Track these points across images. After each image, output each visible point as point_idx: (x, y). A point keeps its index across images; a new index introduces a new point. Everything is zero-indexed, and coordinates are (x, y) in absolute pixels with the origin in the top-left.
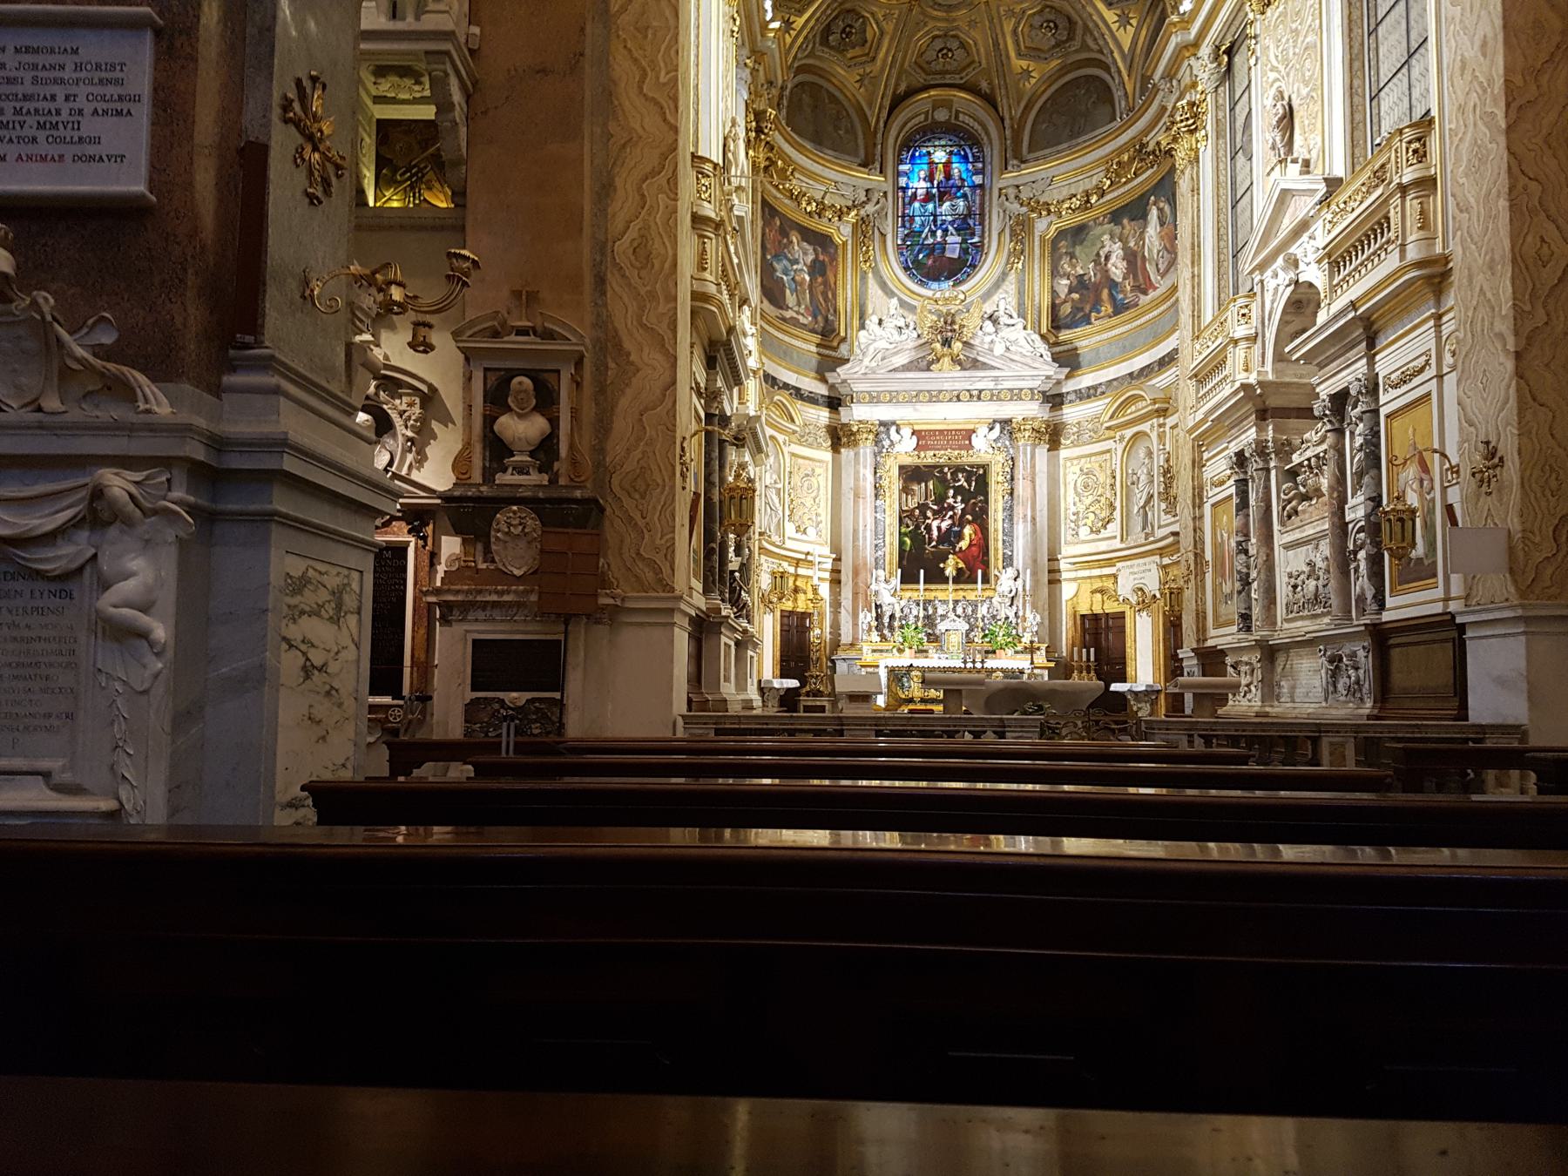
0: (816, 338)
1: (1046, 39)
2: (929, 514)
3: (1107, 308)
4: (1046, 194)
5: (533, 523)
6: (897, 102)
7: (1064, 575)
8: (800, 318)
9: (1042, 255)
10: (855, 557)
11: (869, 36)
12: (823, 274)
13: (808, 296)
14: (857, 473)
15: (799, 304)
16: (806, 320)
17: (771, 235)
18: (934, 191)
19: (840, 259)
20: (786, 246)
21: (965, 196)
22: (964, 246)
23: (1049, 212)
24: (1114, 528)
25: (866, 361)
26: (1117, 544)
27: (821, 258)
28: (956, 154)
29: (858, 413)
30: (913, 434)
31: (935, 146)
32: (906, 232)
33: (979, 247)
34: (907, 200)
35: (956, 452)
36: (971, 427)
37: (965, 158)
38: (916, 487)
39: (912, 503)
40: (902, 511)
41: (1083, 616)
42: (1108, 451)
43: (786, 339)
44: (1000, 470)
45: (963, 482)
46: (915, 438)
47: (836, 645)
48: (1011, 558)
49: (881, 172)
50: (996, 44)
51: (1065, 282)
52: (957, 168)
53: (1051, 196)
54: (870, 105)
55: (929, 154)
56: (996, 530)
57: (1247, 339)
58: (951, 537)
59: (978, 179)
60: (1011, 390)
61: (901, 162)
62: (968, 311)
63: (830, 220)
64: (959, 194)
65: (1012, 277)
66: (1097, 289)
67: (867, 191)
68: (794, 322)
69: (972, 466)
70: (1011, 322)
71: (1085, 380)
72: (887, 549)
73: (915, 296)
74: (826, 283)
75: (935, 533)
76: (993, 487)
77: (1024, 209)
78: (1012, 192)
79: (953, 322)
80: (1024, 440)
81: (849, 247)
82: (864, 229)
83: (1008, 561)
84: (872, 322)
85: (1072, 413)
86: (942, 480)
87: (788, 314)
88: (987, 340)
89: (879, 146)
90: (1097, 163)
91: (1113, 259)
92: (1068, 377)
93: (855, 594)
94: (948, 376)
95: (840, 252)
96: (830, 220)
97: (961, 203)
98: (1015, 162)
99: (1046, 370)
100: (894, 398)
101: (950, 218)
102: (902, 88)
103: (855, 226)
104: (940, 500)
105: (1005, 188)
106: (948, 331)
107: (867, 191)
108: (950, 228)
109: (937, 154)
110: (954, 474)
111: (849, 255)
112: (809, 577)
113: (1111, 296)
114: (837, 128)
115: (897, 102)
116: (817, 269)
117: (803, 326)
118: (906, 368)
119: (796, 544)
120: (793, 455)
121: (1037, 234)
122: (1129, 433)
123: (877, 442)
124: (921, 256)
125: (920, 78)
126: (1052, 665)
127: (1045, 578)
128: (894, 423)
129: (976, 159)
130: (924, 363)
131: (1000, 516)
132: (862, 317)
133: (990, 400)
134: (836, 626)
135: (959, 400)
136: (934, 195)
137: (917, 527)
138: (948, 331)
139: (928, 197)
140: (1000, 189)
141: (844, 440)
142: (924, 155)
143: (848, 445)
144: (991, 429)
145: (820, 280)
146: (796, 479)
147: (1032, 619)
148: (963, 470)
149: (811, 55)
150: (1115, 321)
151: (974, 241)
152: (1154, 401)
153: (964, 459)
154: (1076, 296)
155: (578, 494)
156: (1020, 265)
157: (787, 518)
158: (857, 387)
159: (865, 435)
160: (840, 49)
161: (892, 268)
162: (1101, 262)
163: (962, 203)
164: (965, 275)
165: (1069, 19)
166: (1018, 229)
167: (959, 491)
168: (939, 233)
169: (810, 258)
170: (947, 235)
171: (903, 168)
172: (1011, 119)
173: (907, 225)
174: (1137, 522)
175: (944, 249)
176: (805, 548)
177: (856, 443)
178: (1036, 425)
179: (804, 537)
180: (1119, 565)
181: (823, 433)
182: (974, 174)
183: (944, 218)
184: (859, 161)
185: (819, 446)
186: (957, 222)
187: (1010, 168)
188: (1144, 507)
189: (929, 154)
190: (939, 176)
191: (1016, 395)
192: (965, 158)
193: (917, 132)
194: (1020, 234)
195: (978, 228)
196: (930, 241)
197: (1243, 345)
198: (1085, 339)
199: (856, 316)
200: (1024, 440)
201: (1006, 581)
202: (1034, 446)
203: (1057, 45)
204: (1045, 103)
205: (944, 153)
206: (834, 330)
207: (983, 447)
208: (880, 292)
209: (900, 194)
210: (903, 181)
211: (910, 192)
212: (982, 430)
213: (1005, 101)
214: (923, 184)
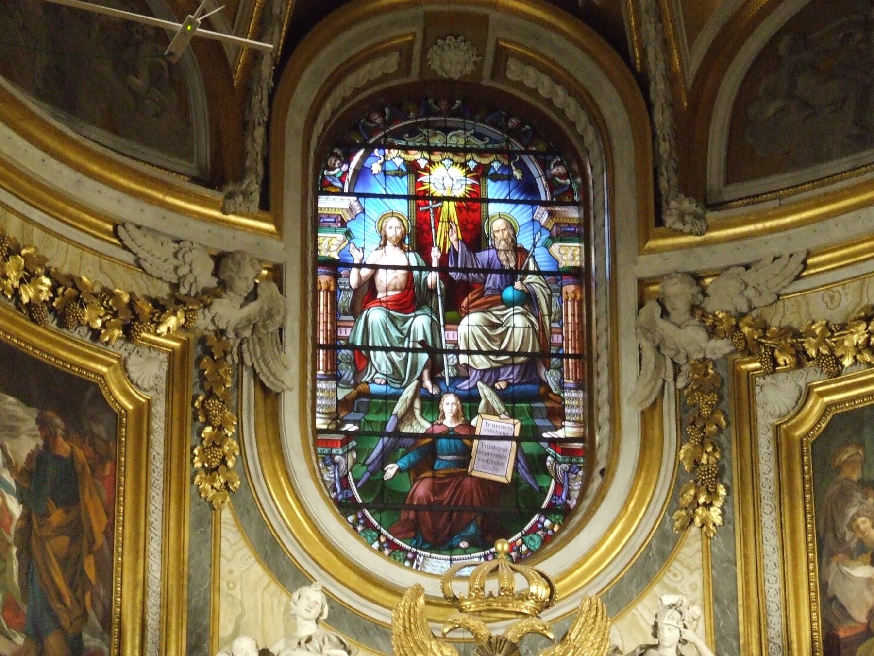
4: (789, 303)
9: (786, 486)
13: (15, 565)
18: (433, 278)
19: (127, 460)
21: (528, 300)
22: (529, 447)
27: (64, 448)
28: (496, 178)
31: (431, 150)
32: (342, 394)
34: (345, 299)
49: (265, 206)
55: (413, 169)
61: (326, 189)
62: (563, 639)
63: (96, 335)
64: (508, 293)
67: (219, 259)
73: (375, 592)
81: (158, 425)
89: (260, 132)
95: (127, 434)
96: (96, 335)
98: (688, 205)
101: (481, 362)
105: (655, 281)
108: (484, 391)
109: (438, 172)
111: (158, 448)
124: (391, 470)
136: (433, 291)
140: (643, 284)
142: (399, 174)
145: (57, 517)
151: (560, 434)
156: (715, 514)
163: (519, 321)
164: (535, 542)
166: (705, 403)
168: (449, 404)
170: (474, 413)
171: (326, 203)
172: (671, 79)
173: (347, 373)
175: (466, 454)
182: (553, 239)
183: (463, 359)
184: (190, 167)
186: (506, 373)
187: (670, 221)
193: (375, 104)
194: (709, 419)
195: (573, 400)
196: (421, 425)
204: (775, 38)
205: (458, 173)
208: (258, 572)
209: (324, 279)
211: (354, 278)
213: (650, 29)
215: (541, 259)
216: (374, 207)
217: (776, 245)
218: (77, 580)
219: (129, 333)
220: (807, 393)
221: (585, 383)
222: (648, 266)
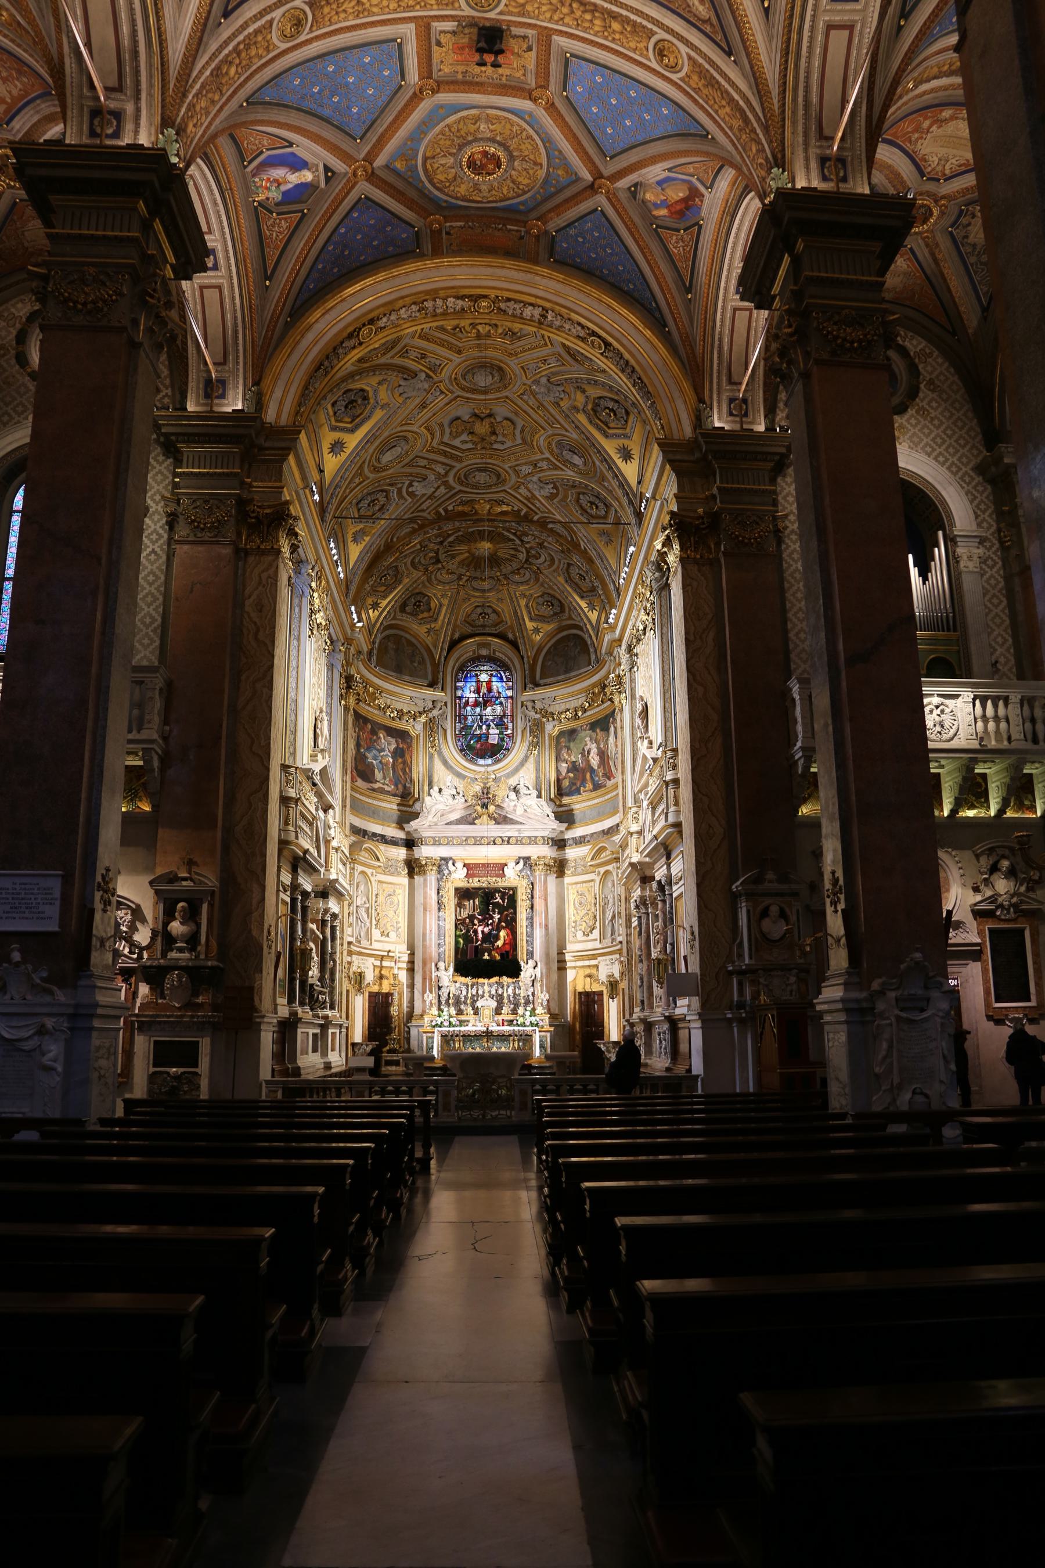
0: (397, 800)
1: (546, 610)
2: (476, 922)
3: (589, 786)
6: (453, 644)
7: (569, 964)
8: (387, 788)
10: (424, 953)
11: (432, 605)
12: (402, 756)
14: (425, 893)
15: (385, 778)
16: (390, 788)
17: (364, 735)
20: (375, 741)
21: (501, 703)
24: (596, 934)
25: (430, 817)
26: (597, 945)
27: (401, 746)
29: (424, 852)
33: (511, 737)
36: (503, 862)
37: (501, 678)
38: (466, 903)
39: (464, 914)
40: (457, 920)
41: (580, 993)
42: (593, 880)
43: (375, 802)
45: (499, 900)
47: (410, 1015)
48: (532, 952)
50: (516, 612)
51: (564, 765)
52: (496, 685)
53: (556, 708)
54: (435, 647)
56: (522, 933)
57: (637, 833)
58: (490, 938)
59: (509, 693)
60: (529, 837)
61: (459, 681)
65: (531, 759)
66: (583, 771)
67: (433, 702)
68: (382, 791)
70: (528, 792)
71: (578, 832)
72: (447, 947)
74: (404, 763)
75: (480, 935)
77: (538, 716)
78: (529, 704)
79: (488, 793)
80: (539, 873)
82: (432, 727)
83: (530, 954)
84: (435, 791)
85: (572, 853)
87: (376, 786)
88: (511, 805)
90: (581, 691)
91: (592, 754)
92: (567, 829)
93: (424, 979)
94: (486, 828)
95: (415, 741)
97: (498, 709)
99: (551, 826)
100: (450, 842)
102: (457, 636)
103: (425, 724)
106: (485, 798)
107: (433, 702)
112: (392, 968)
113: (591, 777)
114: (412, 662)
115: (453, 644)
116: (398, 753)
117: (388, 793)
118: (459, 821)
119: (380, 945)
120: (379, 881)
121: (547, 732)
122: (602, 870)
123: (440, 871)
125: (469, 630)
126: (552, 1029)
127: (555, 966)
128: (451, 858)
129: (508, 680)
130: (469, 820)
131: (525, 923)
132: (430, 786)
134: (412, 1001)
135: (495, 844)
137: (468, 931)
138: (485, 798)
139: (476, 704)
141: (417, 870)
143: (419, 874)
145: (400, 760)
146: (381, 898)
147: (543, 997)
148: (499, 891)
149: (394, 618)
150: (594, 794)
152: (613, 853)
153: (500, 884)
154: (571, 775)
158: (425, 834)
160: (414, 614)
161: (451, 751)
162: (586, 754)
165: (560, 601)
166: (535, 728)
167: (496, 905)
168: (484, 727)
169: (393, 747)
172: (528, 657)
174: (609, 930)
175: (487, 738)
176: (387, 947)
179: (387, 939)
180: (600, 959)
181: (401, 864)
185: (399, 874)
189: (477, 675)
190: (484, 690)
191: (533, 841)
192: (501, 678)
195: (510, 725)
196: (478, 732)
197: (635, 836)
198: (579, 804)
199: (426, 784)
200: (539, 873)
201: (527, 972)
202: (546, 875)
203: (555, 614)
206: (410, 794)
207: (512, 876)
208: (443, 767)
210: (459, 693)
212: (511, 864)
214: (473, 695)
215: (504, 694)
216: (468, 685)
217: (548, 695)
218: (404, 772)
221: (512, 722)
222: (523, 699)
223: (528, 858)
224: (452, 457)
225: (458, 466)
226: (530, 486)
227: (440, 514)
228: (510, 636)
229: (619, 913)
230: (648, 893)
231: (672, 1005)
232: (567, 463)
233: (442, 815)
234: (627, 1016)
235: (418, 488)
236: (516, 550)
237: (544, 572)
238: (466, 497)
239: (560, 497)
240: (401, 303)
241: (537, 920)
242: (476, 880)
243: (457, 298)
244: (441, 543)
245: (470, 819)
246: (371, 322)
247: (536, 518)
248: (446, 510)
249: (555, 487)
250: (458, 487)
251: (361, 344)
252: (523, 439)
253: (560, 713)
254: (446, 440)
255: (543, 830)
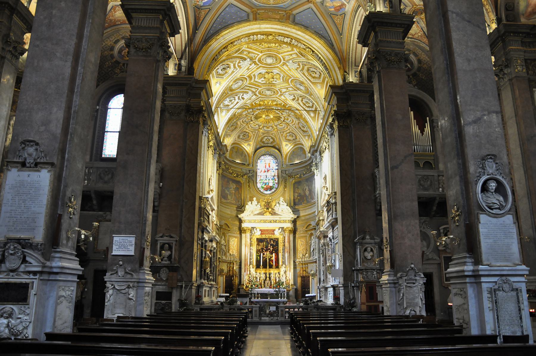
2: (264, 250)
5: (167, 270)
8: (232, 202)
14: (246, 240)
15: (231, 198)
22: (274, 183)
23: (293, 178)
24: (307, 255)
30: (260, 230)
34: (260, 172)
35: (271, 235)
39: (260, 248)
40: (257, 250)
44: (281, 240)
45: (272, 243)
46: (260, 232)
51: (296, 194)
67: (249, 171)
69: (274, 239)
70: (283, 204)
76: (280, 244)
78: (284, 172)
86: (267, 242)
87: (228, 201)
88: (277, 209)
94: (268, 217)
104: (267, 247)
110: (270, 241)
117: (233, 204)
122: (310, 232)
123: (251, 232)
125: (263, 145)
128: (255, 227)
133: (279, 222)
135: (271, 222)
141: (243, 231)
143: (243, 233)
144: (279, 230)
145: (237, 192)
148: (272, 240)
154: (299, 198)
155: (175, 265)
157: (227, 252)
159: (248, 231)
162: (304, 190)
165: (296, 136)
167: (271, 245)
169: (235, 186)
177: (246, 233)
178: (290, 229)
188: (313, 251)
191: (285, 221)
196: (265, 181)
202: (289, 234)
203: (294, 139)
207: (277, 234)
212: (277, 230)
219: (242, 177)
220: (293, 180)
223: (283, 228)
224: (258, 86)
225: (260, 89)
226: (285, 96)
227: (253, 105)
228: (277, 147)
229: (316, 248)
230: (326, 241)
231: (334, 281)
232: (299, 89)
233: (252, 212)
234: (318, 285)
235: (245, 96)
236: (280, 117)
237: (290, 125)
238: (262, 99)
239: (296, 99)
240: (242, 37)
241: (286, 250)
242: (264, 235)
243: (261, 35)
244: (253, 114)
245: (262, 213)
246: (232, 43)
247: (287, 107)
248: (255, 103)
249: (294, 96)
250: (260, 96)
251: (228, 50)
252: (283, 80)
253: (295, 175)
254: (255, 80)
255: (289, 217)
